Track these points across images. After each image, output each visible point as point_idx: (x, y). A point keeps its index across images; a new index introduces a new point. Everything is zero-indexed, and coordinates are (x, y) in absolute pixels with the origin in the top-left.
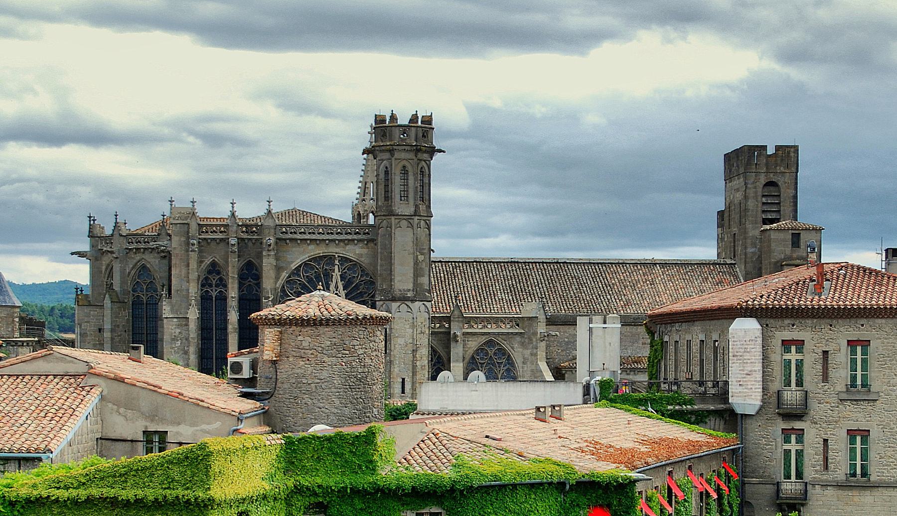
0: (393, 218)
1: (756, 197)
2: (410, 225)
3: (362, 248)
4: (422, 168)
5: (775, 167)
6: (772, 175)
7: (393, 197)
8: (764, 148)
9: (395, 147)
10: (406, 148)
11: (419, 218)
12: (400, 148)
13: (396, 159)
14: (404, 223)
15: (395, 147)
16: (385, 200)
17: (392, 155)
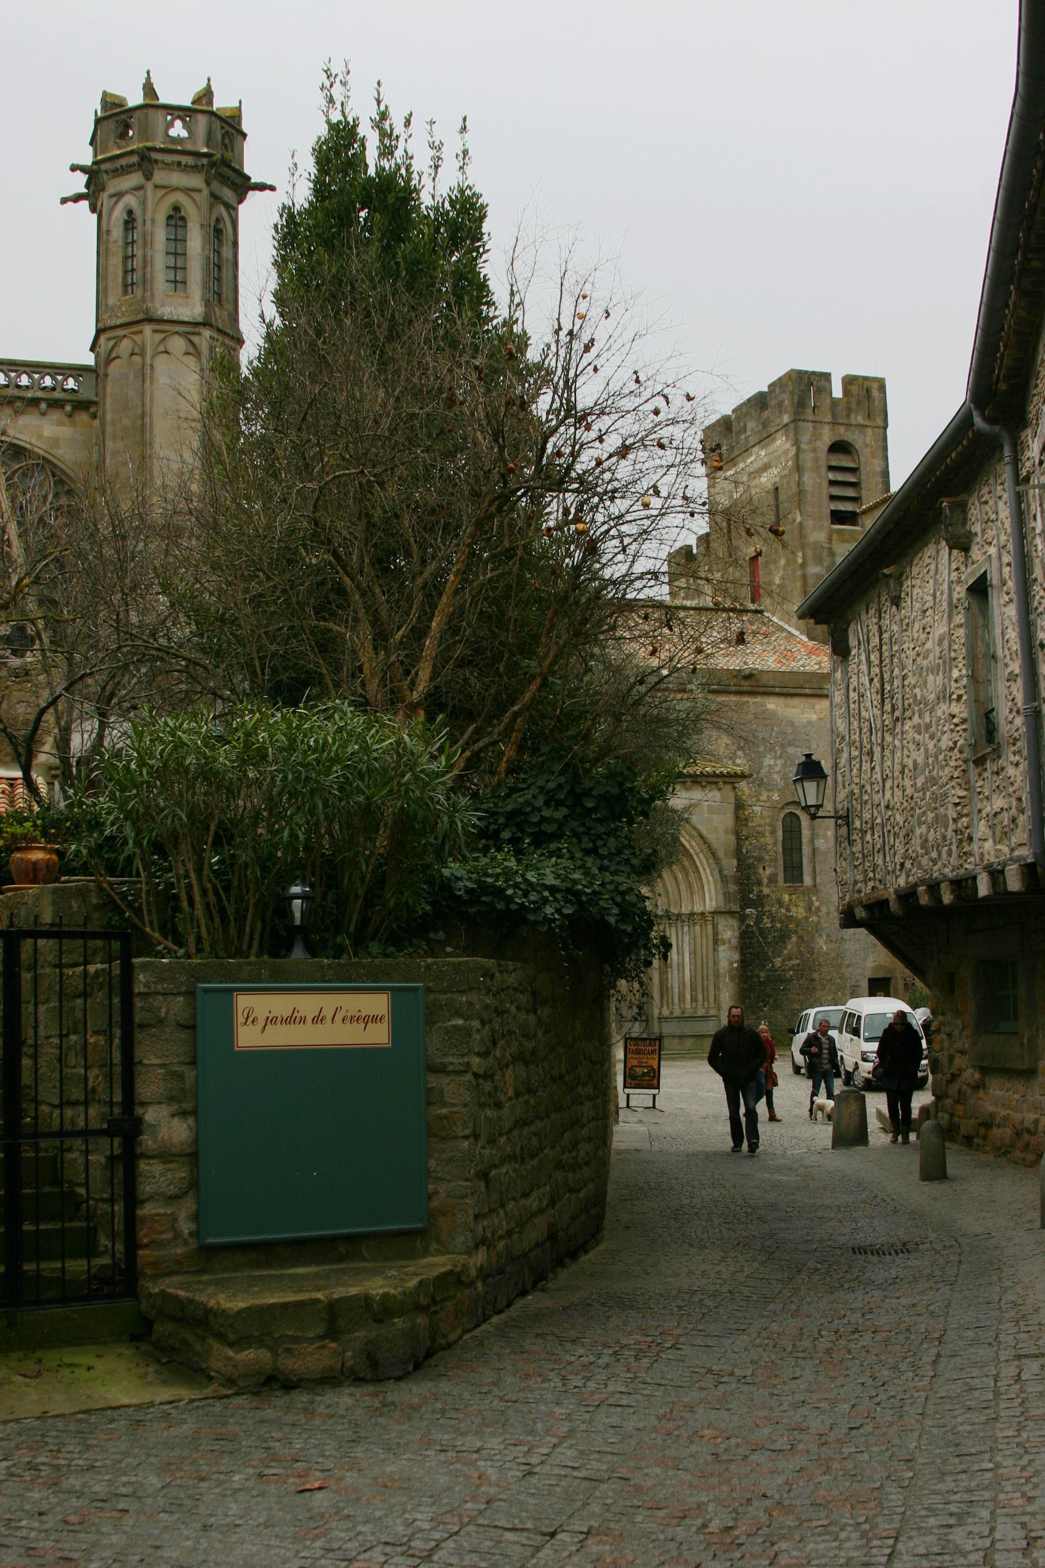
0: (148, 329)
1: (816, 469)
2: (191, 350)
3: (59, 423)
4: (218, 221)
5: (848, 415)
6: (842, 429)
7: (148, 275)
8: (826, 377)
9: (155, 156)
10: (185, 160)
11: (215, 335)
12: (169, 158)
13: (156, 187)
14: (178, 344)
15: (155, 156)
16: (125, 293)
17: (148, 177)
